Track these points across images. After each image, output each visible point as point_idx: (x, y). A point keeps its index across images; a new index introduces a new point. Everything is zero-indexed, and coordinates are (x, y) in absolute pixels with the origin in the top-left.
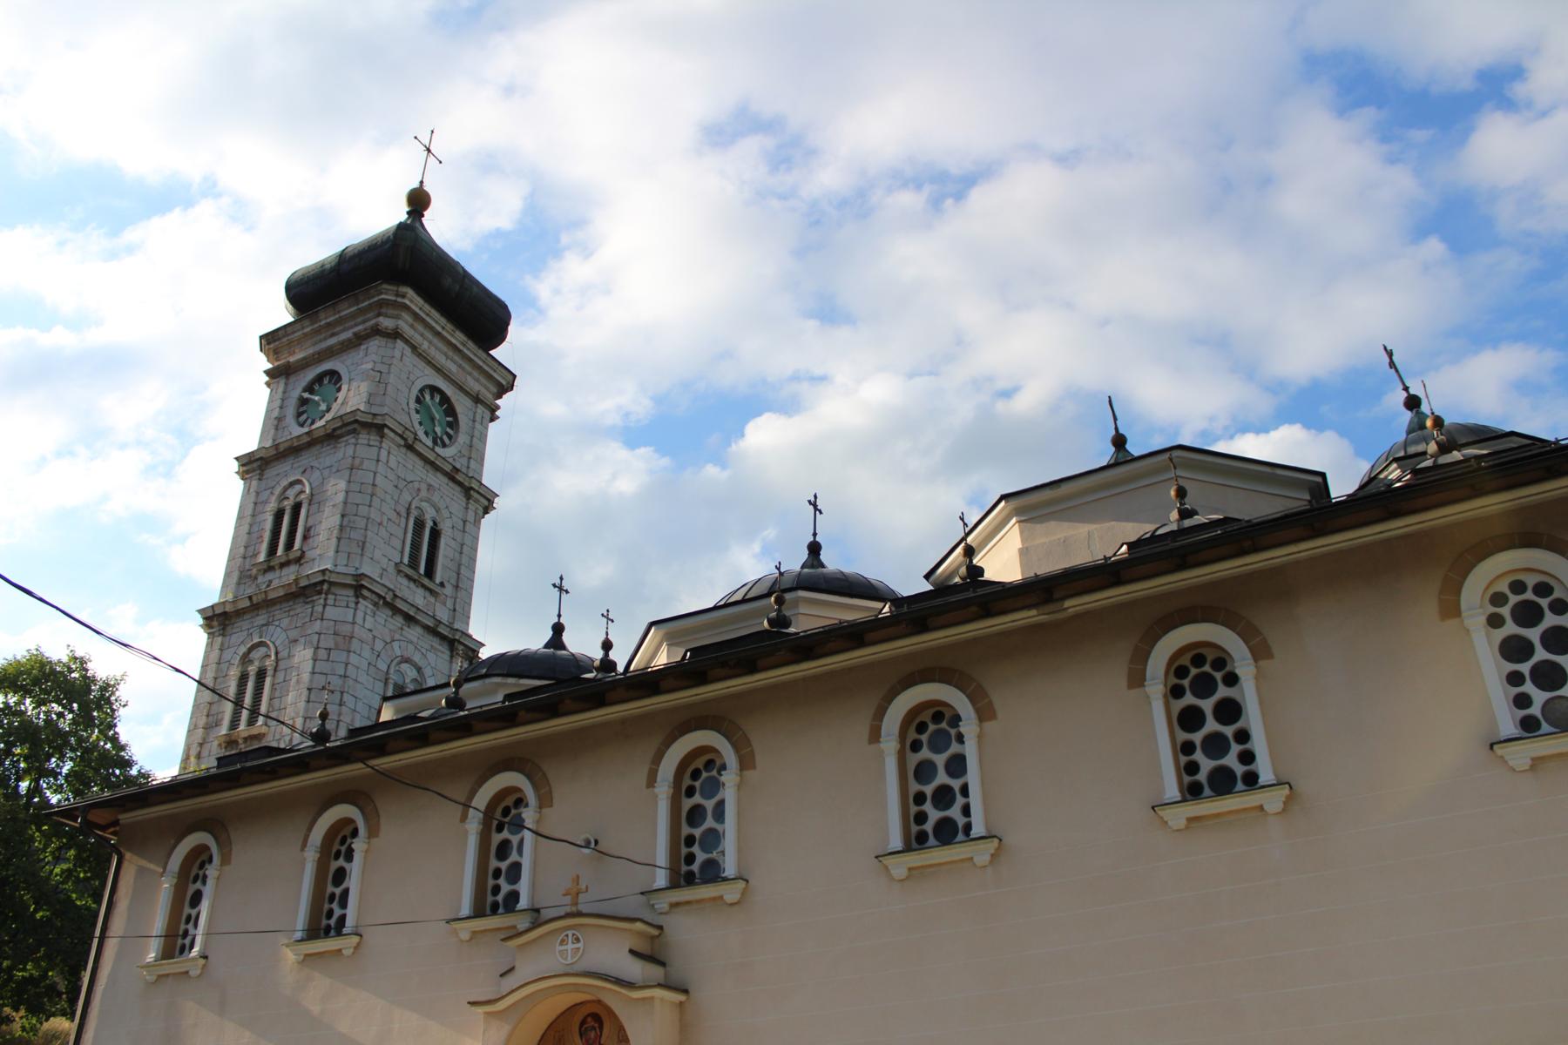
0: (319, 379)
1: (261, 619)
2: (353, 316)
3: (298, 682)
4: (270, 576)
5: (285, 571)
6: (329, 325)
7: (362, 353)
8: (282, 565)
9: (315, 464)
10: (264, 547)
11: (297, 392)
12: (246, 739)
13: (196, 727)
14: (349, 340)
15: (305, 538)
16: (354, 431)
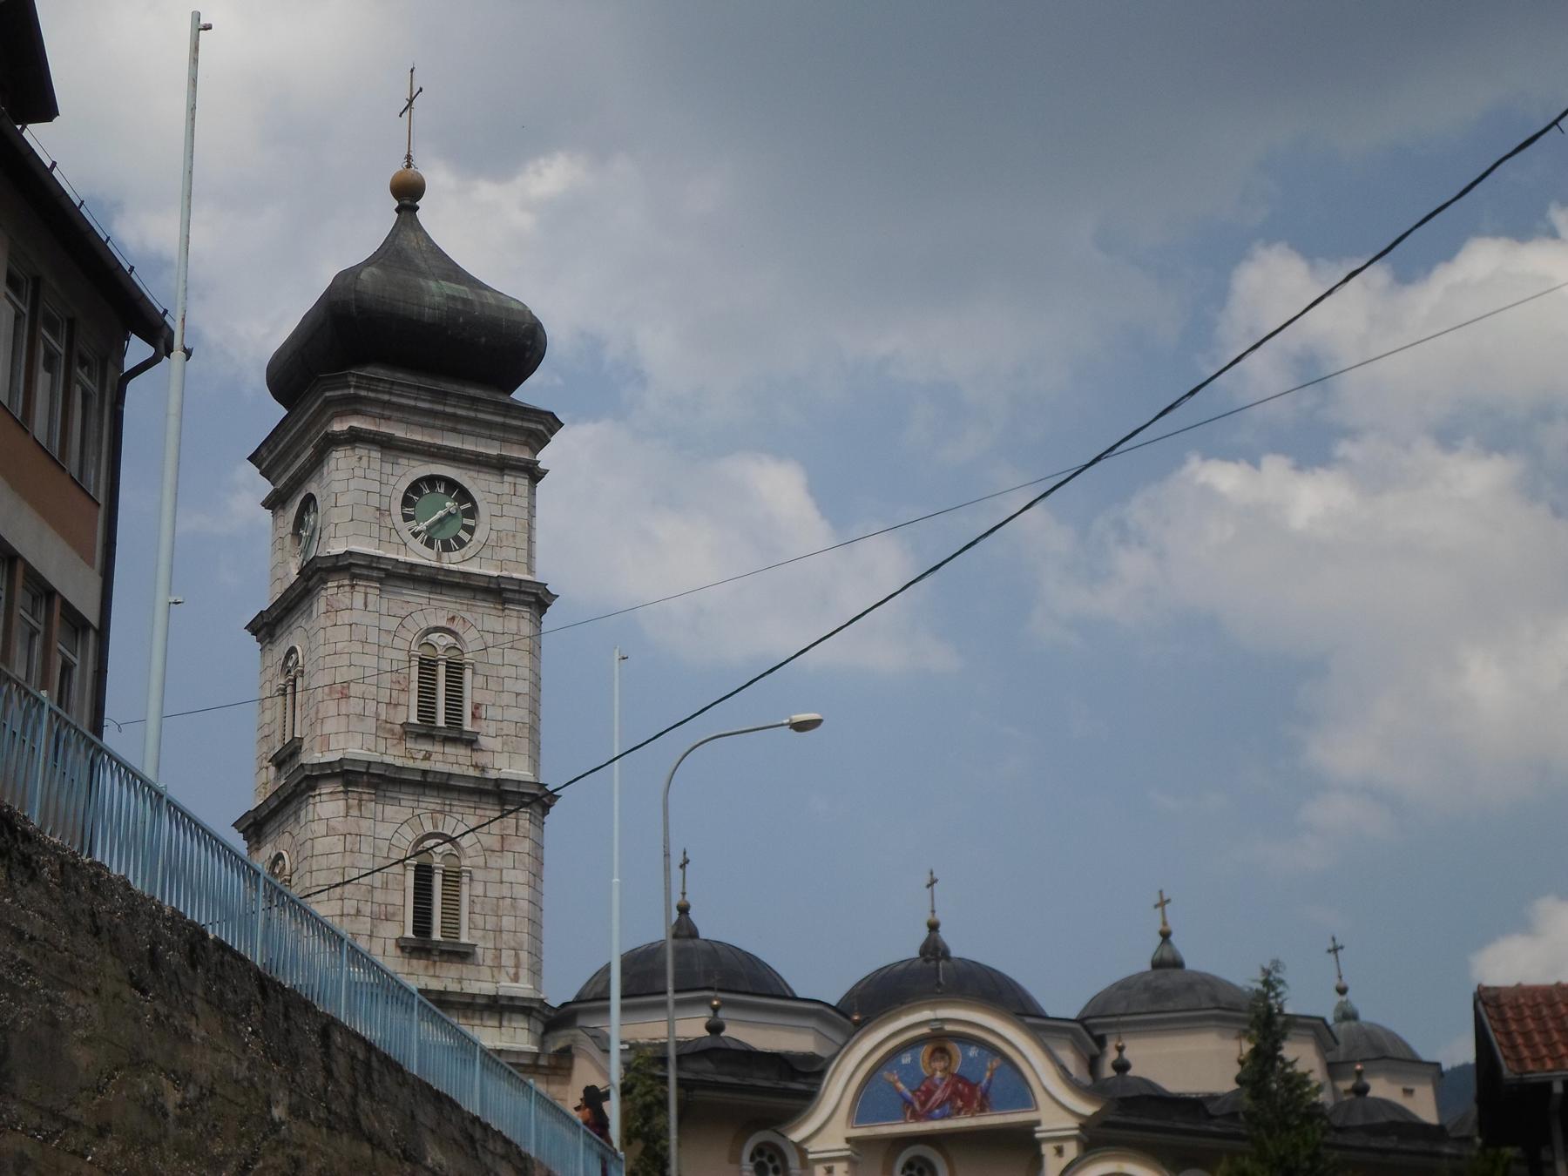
0: (432, 481)
1: (431, 802)
2: (489, 425)
3: (513, 907)
4: (426, 746)
5: (449, 749)
6: (454, 415)
7: (506, 488)
8: (446, 740)
9: (467, 616)
10: (414, 700)
11: (404, 485)
12: (442, 952)
13: (358, 911)
14: (488, 456)
15: (473, 715)
16: (528, 604)
